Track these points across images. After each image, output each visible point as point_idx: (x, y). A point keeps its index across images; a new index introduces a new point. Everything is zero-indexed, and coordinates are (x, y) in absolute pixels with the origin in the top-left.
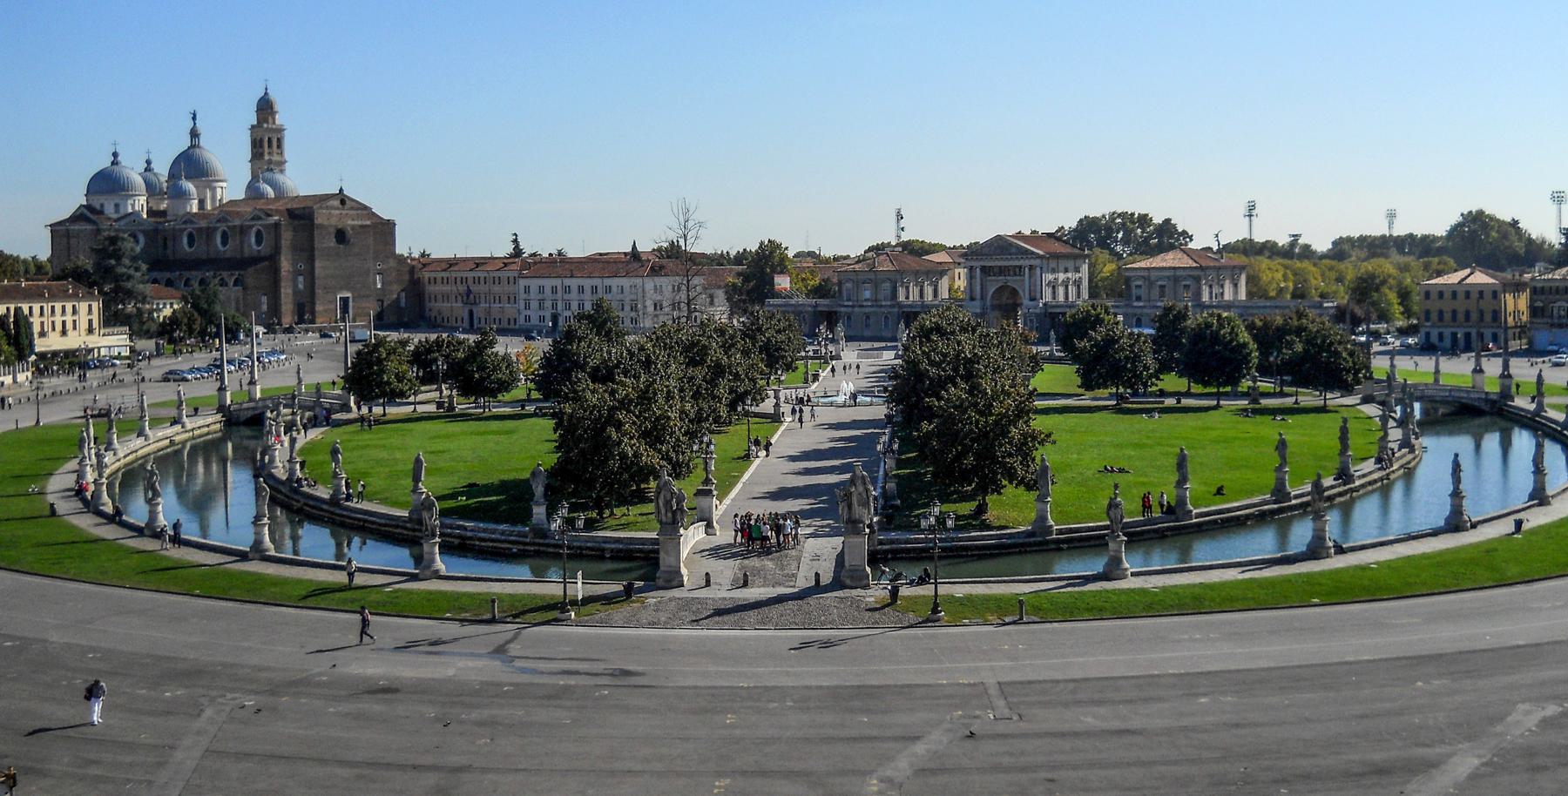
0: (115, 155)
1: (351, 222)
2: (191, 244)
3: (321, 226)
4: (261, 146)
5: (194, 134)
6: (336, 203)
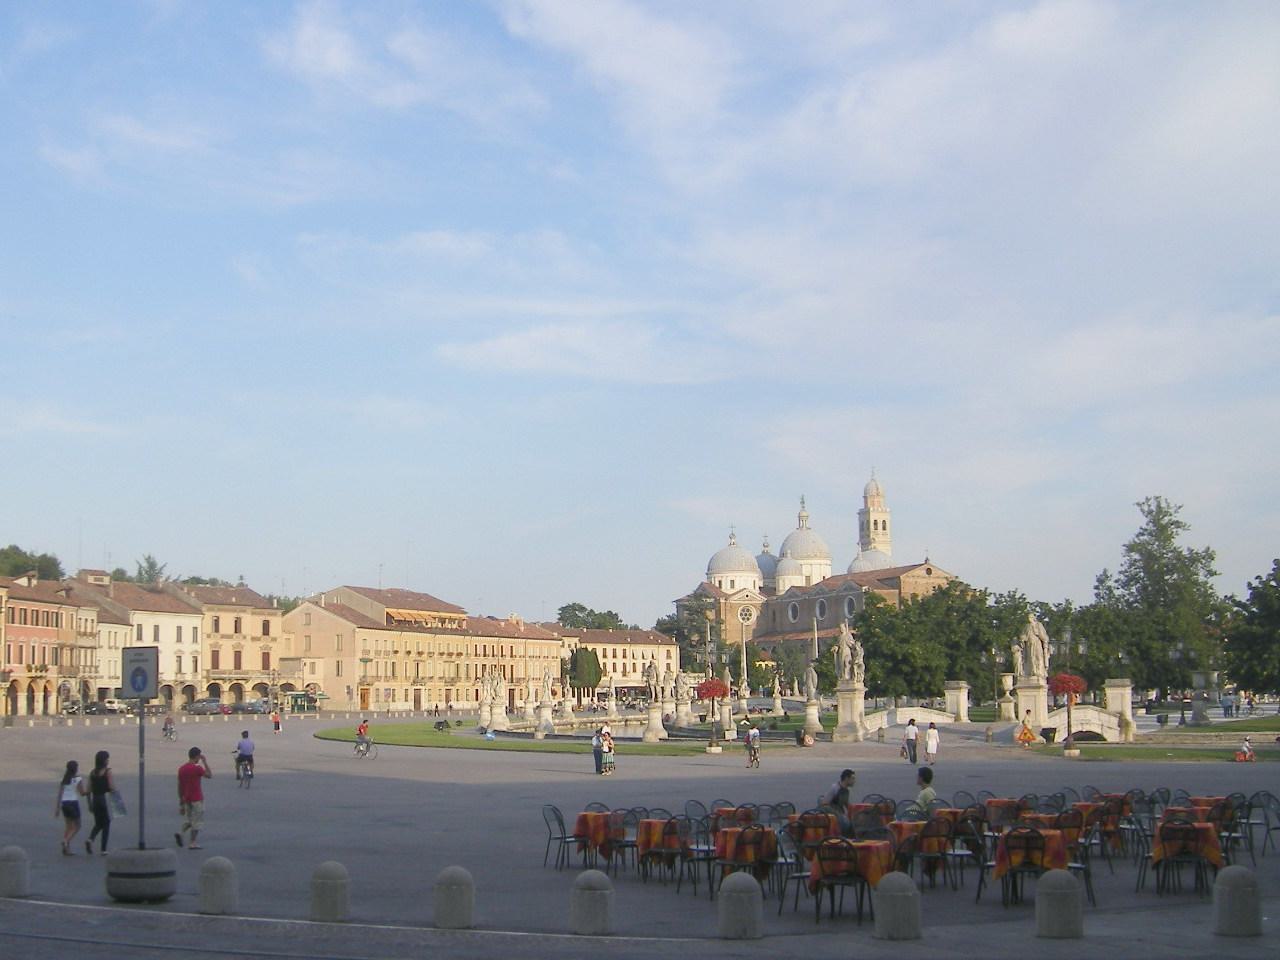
2: (795, 618)
4: (868, 528)
6: (923, 572)
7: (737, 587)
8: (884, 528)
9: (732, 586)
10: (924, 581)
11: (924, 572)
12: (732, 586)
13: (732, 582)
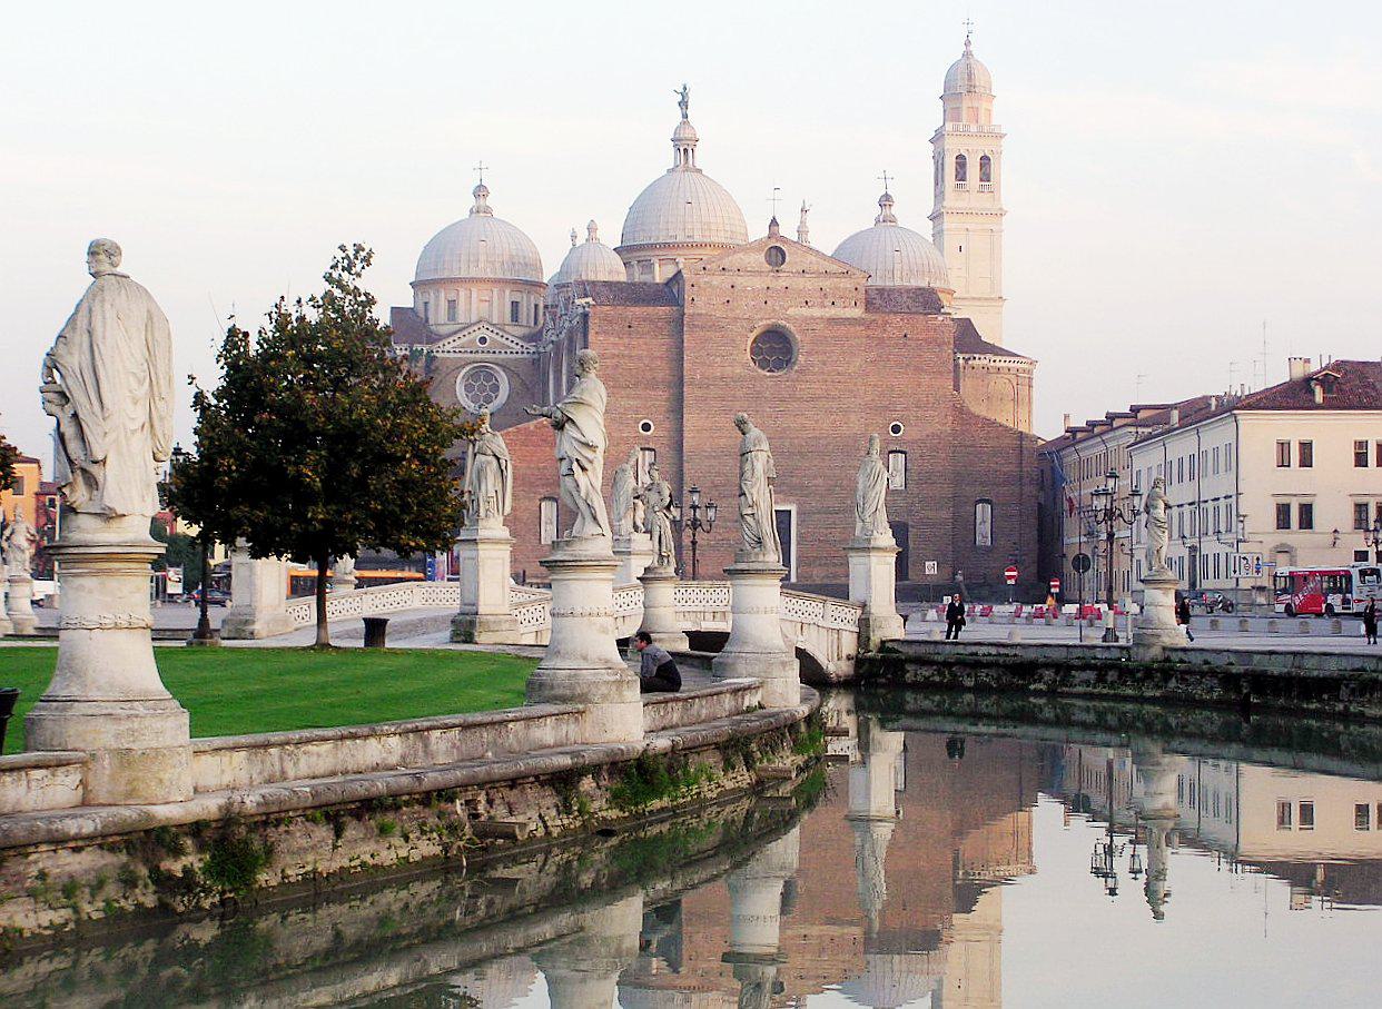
0: (480, 191)
1: (792, 315)
3: (715, 326)
5: (684, 146)
6: (759, 259)
7: (462, 318)
8: (985, 177)
9: (452, 316)
10: (759, 283)
11: (761, 257)
12: (452, 316)
13: (452, 304)
